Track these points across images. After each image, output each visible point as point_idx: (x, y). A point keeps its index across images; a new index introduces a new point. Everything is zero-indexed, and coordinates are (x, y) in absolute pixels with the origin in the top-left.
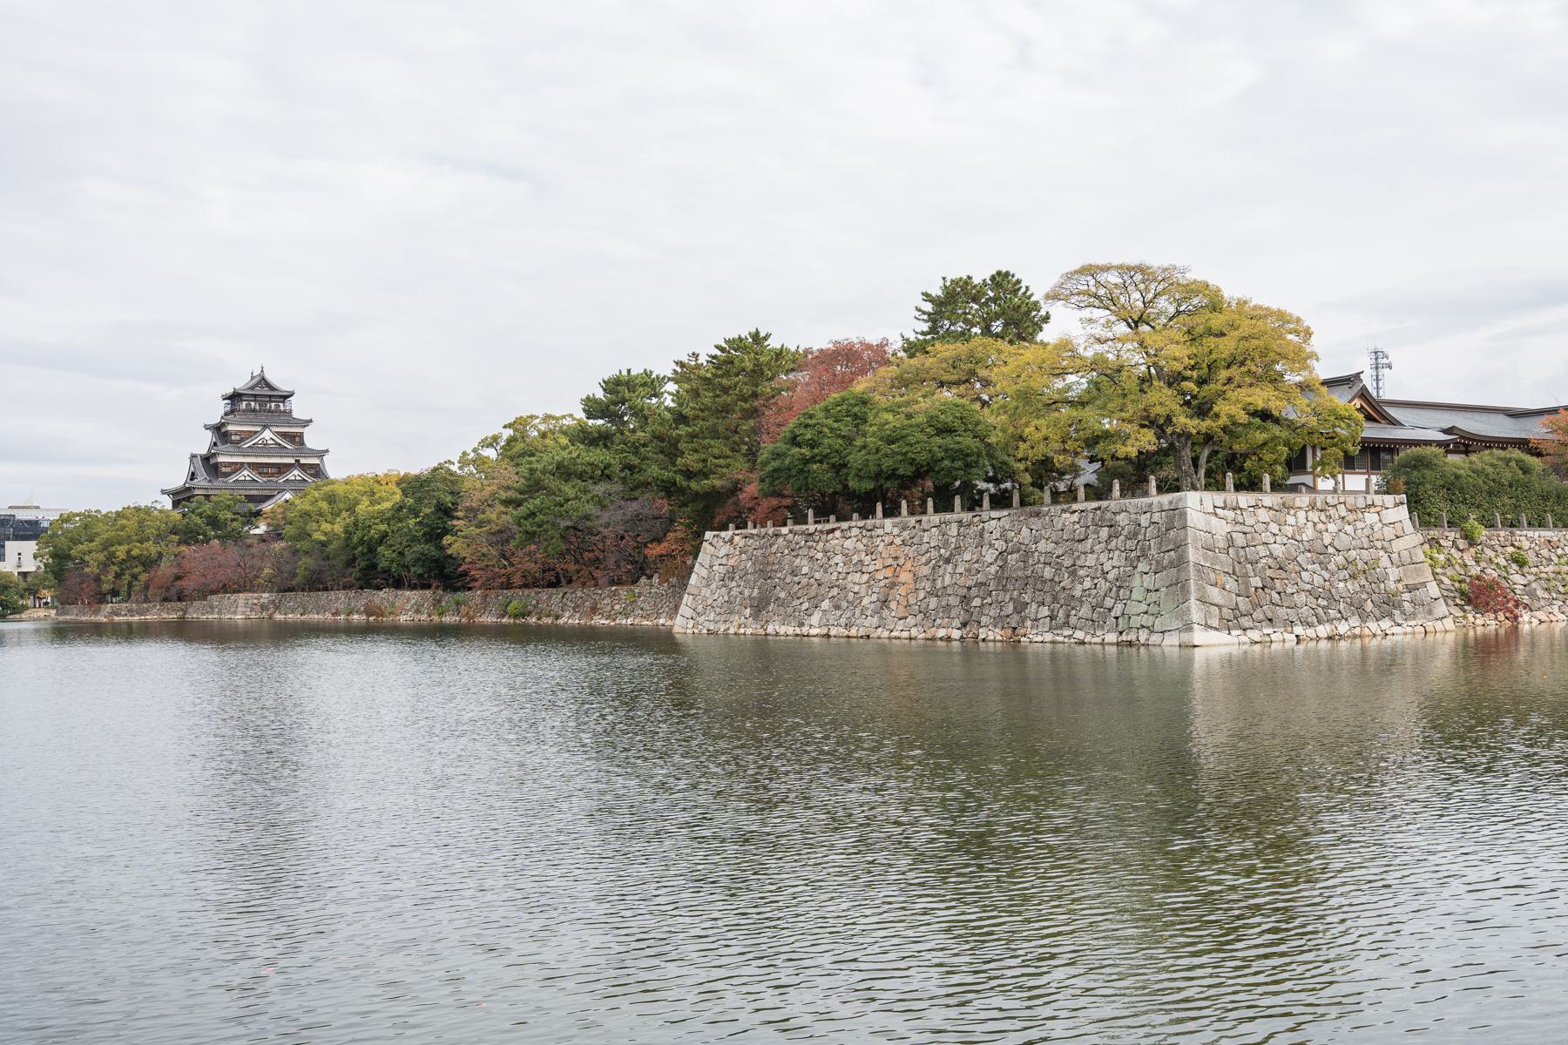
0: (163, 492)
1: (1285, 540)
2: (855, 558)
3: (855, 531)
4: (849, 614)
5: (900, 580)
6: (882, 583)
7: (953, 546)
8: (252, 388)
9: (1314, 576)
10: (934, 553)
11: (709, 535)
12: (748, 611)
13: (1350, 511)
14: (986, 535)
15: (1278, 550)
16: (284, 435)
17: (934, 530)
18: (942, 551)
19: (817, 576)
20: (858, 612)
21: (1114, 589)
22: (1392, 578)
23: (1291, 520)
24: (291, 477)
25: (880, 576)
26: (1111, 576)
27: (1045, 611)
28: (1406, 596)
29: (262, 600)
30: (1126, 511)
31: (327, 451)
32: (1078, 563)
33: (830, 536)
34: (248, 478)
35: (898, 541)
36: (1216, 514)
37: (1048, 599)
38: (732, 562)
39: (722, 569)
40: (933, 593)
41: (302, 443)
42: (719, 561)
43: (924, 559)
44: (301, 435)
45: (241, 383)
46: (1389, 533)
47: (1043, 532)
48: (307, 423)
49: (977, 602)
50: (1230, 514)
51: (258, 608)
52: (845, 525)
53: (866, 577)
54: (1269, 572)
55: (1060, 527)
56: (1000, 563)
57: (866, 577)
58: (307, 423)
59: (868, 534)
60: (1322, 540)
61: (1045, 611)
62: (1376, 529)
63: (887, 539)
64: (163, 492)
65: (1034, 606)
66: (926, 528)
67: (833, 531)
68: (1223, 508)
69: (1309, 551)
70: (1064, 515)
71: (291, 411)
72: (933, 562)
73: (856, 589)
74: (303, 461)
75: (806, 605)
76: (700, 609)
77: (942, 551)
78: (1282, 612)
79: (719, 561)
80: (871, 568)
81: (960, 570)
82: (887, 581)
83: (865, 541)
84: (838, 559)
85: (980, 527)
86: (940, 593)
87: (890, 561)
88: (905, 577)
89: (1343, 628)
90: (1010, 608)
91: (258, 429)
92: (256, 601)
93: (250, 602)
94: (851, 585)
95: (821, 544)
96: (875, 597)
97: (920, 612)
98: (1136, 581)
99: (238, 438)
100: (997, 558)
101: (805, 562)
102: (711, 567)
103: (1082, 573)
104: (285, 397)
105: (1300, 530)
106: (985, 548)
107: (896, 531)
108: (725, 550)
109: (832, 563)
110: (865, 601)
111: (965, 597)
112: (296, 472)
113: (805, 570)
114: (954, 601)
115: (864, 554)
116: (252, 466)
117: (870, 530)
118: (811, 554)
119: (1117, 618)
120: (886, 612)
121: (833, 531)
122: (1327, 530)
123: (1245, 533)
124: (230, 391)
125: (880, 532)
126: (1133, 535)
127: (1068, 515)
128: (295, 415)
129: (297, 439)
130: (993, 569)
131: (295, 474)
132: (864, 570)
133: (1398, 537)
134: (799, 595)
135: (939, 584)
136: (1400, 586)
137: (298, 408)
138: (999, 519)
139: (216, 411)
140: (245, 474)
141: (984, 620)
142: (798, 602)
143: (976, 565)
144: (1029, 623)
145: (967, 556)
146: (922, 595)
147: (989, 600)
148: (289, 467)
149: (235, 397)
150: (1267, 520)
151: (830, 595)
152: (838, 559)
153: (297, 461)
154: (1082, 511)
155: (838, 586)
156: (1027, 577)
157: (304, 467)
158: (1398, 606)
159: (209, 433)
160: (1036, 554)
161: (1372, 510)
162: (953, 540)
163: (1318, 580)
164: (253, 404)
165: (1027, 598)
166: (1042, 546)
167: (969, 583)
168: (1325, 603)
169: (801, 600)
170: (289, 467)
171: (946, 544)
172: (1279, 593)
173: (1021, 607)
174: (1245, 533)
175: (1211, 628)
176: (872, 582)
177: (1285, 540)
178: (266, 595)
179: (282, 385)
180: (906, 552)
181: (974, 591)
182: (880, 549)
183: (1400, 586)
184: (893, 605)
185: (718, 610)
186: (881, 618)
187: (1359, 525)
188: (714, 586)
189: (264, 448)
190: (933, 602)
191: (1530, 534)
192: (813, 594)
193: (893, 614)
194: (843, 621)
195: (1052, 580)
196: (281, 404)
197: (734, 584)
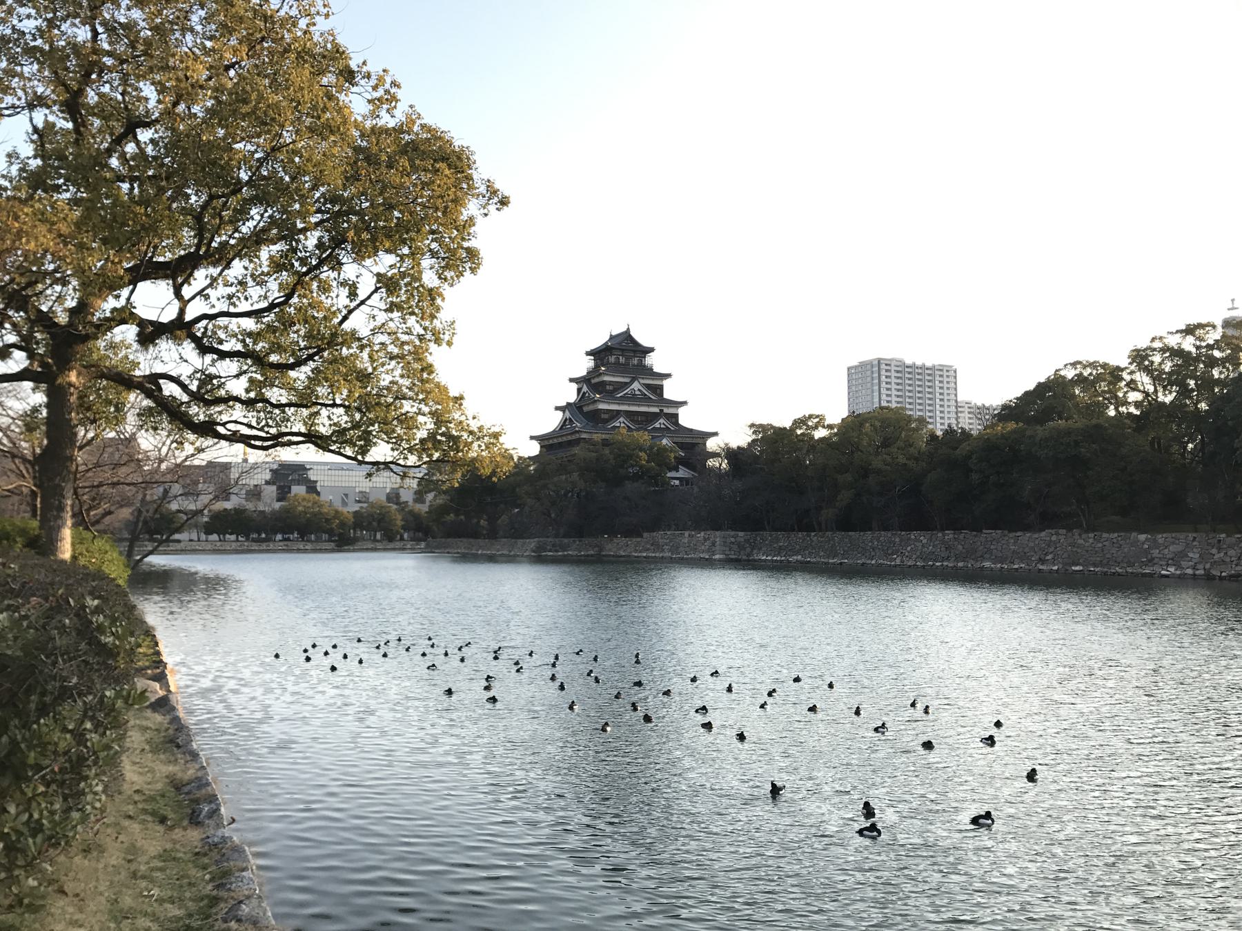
0: (532, 438)
8: (620, 344)
16: (648, 387)
24: (657, 425)
31: (684, 403)
41: (661, 394)
44: (661, 388)
45: (599, 340)
48: (668, 376)
51: (735, 547)
58: (668, 376)
64: (532, 438)
74: (666, 410)
91: (627, 380)
92: (733, 540)
93: (728, 541)
99: (611, 388)
112: (662, 421)
116: (629, 414)
129: (658, 391)
137: (656, 362)
139: (584, 365)
140: (621, 422)
149: (596, 354)
153: (662, 411)
159: (574, 386)
170: (655, 417)
178: (741, 534)
179: (643, 339)
189: (633, 398)
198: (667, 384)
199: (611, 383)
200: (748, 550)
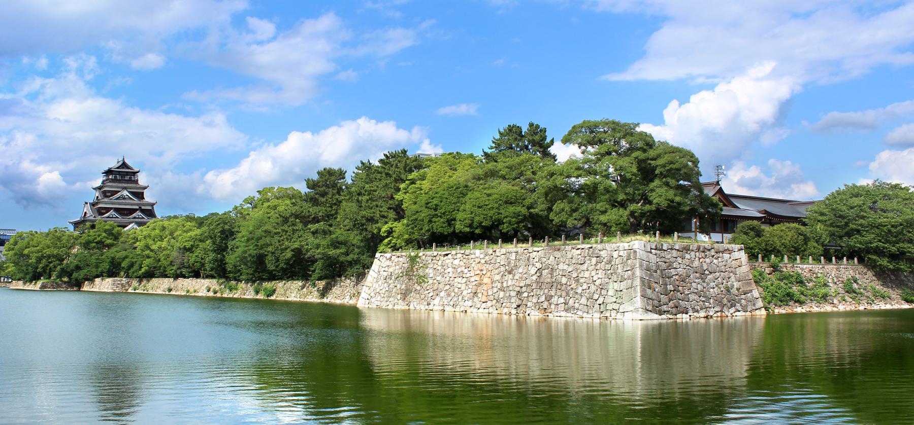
2: (459, 270)
3: (459, 256)
4: (456, 299)
5: (483, 282)
6: (474, 284)
7: (513, 265)
8: (118, 168)
10: (502, 269)
11: (378, 255)
12: (399, 297)
14: (531, 260)
17: (503, 256)
18: (507, 267)
19: (438, 278)
20: (460, 298)
21: (599, 290)
23: (687, 256)
25: (472, 279)
26: (597, 283)
27: (562, 300)
29: (122, 282)
30: (606, 249)
32: (580, 276)
33: (446, 257)
34: (114, 216)
35: (483, 261)
36: (651, 252)
37: (564, 294)
38: (391, 270)
39: (386, 274)
40: (501, 289)
42: (384, 269)
43: (497, 271)
44: (143, 193)
47: (562, 259)
49: (525, 295)
52: (454, 252)
53: (465, 280)
54: (677, 283)
55: (570, 256)
56: (538, 274)
57: (465, 280)
59: (467, 257)
61: (562, 300)
63: (479, 260)
65: (556, 297)
66: (498, 255)
67: (447, 255)
68: (655, 249)
70: (573, 251)
71: (137, 180)
72: (502, 273)
73: (459, 286)
75: (431, 294)
76: (372, 294)
77: (507, 267)
79: (384, 269)
80: (468, 276)
81: (517, 277)
82: (476, 282)
83: (465, 261)
84: (450, 270)
85: (527, 255)
86: (505, 289)
87: (478, 272)
88: (486, 280)
90: (543, 299)
92: (119, 282)
94: (456, 284)
95: (440, 262)
96: (469, 291)
97: (494, 299)
98: (611, 286)
99: (109, 194)
100: (537, 272)
101: (431, 271)
102: (379, 272)
103: (582, 281)
104: (135, 173)
105: (692, 262)
106: (530, 266)
107: (482, 256)
108: (388, 263)
109: (446, 271)
110: (465, 293)
111: (519, 292)
113: (431, 275)
114: (513, 294)
115: (464, 267)
117: (467, 255)
118: (435, 267)
119: (600, 305)
120: (476, 299)
121: (447, 255)
122: (705, 262)
123: (665, 263)
124: (107, 169)
125: (473, 256)
126: (609, 262)
127: (575, 250)
128: (139, 182)
129: (140, 196)
130: (534, 278)
131: (138, 213)
132: (464, 276)
133: (740, 266)
134: (428, 288)
135: (505, 285)
137: (142, 180)
138: (538, 251)
141: (529, 304)
142: (427, 292)
143: (525, 275)
144: (553, 306)
145: (520, 270)
146: (495, 290)
147: (532, 294)
148: (135, 210)
149: (108, 172)
151: (445, 289)
152: (450, 270)
154: (583, 249)
155: (450, 284)
156: (553, 282)
157: (143, 211)
160: (558, 270)
162: (513, 262)
163: (700, 287)
164: (118, 176)
165: (553, 293)
166: (561, 266)
167: (522, 285)
168: (704, 299)
169: (429, 291)
171: (509, 263)
172: (681, 294)
173: (549, 298)
174: (665, 263)
175: (648, 310)
176: (468, 283)
177: (685, 267)
180: (487, 267)
181: (524, 289)
182: (473, 265)
184: (480, 295)
185: (382, 295)
186: (473, 301)
188: (380, 283)
190: (502, 294)
191: (801, 266)
192: (435, 288)
193: (480, 300)
194: (452, 303)
195: (566, 284)
196: (133, 177)
197: (392, 281)
198: (145, 191)
199: (109, 191)
200: (127, 288)
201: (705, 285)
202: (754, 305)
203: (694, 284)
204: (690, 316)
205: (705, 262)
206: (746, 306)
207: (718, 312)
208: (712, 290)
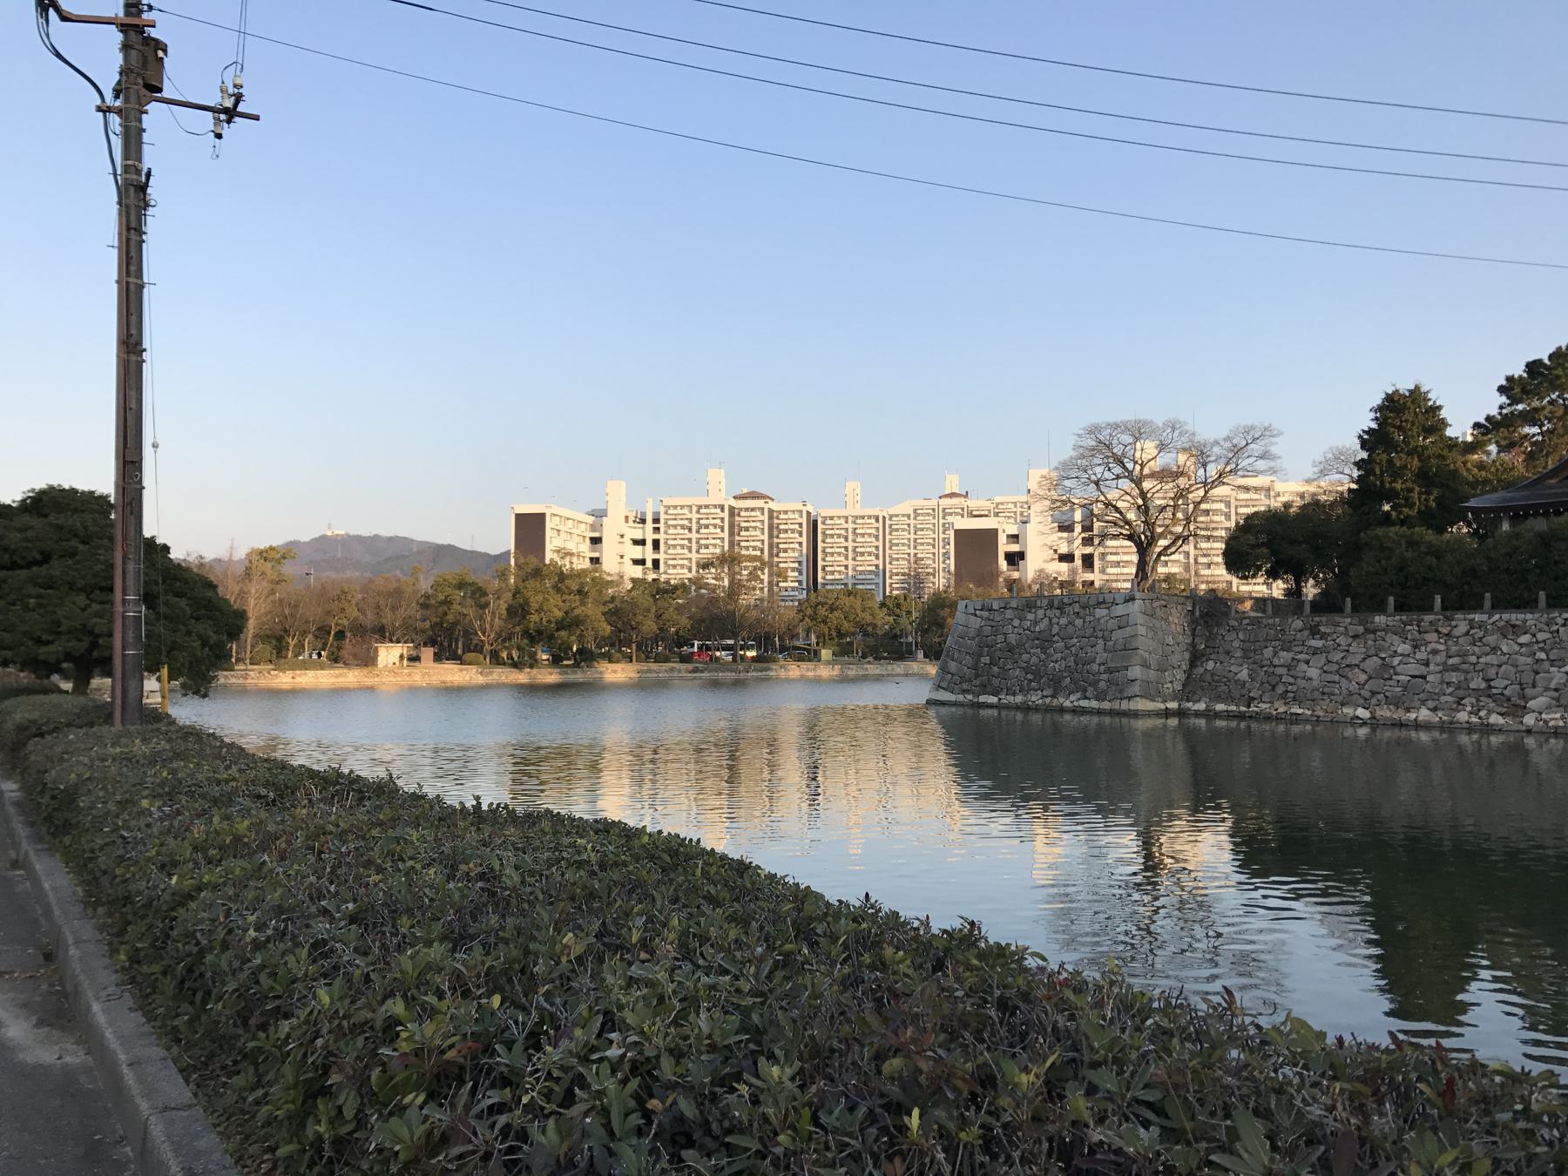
1: (1021, 631)
9: (1033, 656)
13: (1084, 608)
15: (1012, 638)
22: (1098, 661)
23: (1031, 616)
28: (1105, 676)
36: (976, 615)
46: (1112, 624)
50: (985, 614)
60: (1051, 630)
62: (1102, 621)
69: (1038, 639)
78: (996, 682)
89: (1035, 698)
133: (1120, 628)
136: (1102, 667)
150: (1012, 617)
158: (1095, 684)
161: (1102, 606)
163: (1034, 660)
177: (1021, 631)
183: (1102, 667)
187: (1088, 619)
201: (1043, 656)
202: (1121, 691)
203: (1025, 657)
204: (1000, 699)
205: (1058, 624)
206: (1105, 692)
207: (1047, 697)
208: (1052, 664)
